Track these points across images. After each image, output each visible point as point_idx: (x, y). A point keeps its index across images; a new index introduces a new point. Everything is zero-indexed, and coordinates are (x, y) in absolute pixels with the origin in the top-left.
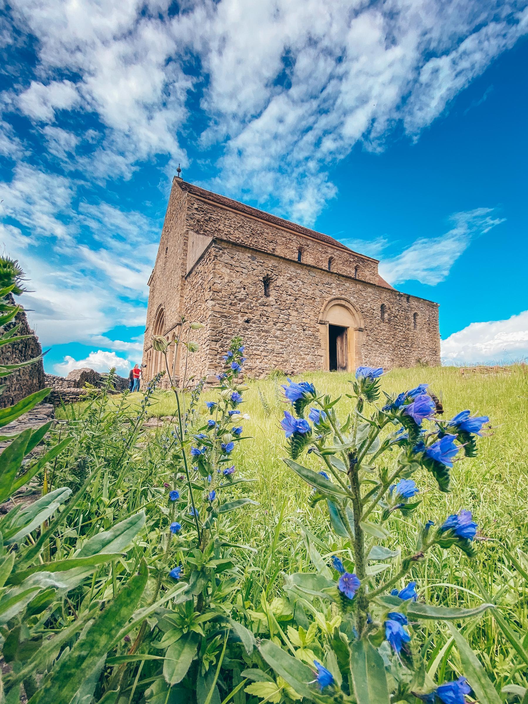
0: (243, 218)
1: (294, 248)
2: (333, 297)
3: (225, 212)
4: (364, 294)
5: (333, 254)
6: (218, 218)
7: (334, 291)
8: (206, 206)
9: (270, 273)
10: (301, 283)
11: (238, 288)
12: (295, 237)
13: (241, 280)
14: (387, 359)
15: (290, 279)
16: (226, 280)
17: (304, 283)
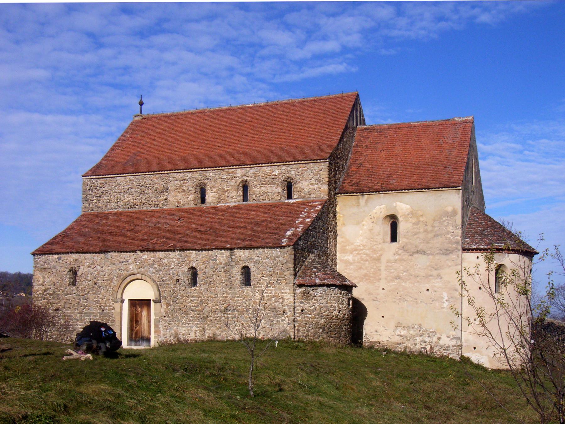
0: (131, 178)
1: (191, 188)
2: (129, 273)
3: (115, 179)
4: (165, 261)
5: (245, 175)
6: (110, 188)
7: (131, 267)
8: (99, 181)
9: (73, 266)
10: (99, 267)
11: (49, 285)
12: (190, 175)
13: (51, 279)
14: (194, 328)
15: (89, 267)
16: (41, 282)
17: (102, 267)
